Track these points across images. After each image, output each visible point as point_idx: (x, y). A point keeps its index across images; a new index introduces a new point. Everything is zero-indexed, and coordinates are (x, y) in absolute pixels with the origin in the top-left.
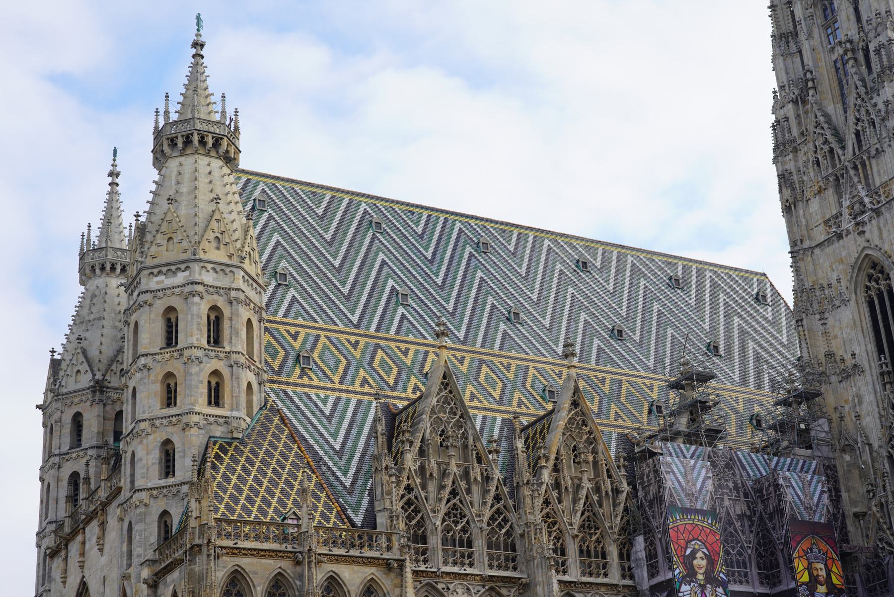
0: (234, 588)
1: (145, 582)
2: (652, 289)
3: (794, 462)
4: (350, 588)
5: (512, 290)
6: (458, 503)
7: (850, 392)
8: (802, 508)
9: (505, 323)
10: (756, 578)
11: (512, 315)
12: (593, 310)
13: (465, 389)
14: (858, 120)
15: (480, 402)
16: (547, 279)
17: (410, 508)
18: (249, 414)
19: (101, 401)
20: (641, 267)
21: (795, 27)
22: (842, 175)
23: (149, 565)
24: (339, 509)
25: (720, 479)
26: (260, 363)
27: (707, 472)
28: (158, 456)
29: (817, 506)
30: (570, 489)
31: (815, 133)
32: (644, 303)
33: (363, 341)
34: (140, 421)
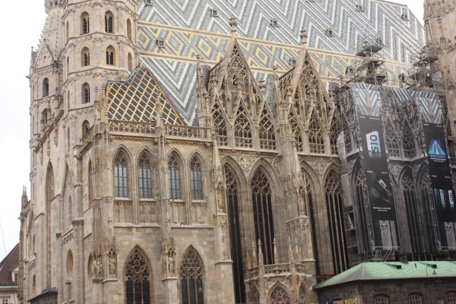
0: (121, 157)
1: (75, 156)
3: (424, 94)
4: (184, 157)
5: (273, 10)
6: (243, 114)
7: (453, 58)
8: (428, 117)
9: (269, 27)
10: (403, 153)
11: (273, 22)
12: (316, 21)
13: (248, 59)
15: (256, 65)
16: (292, 5)
17: (217, 116)
18: (130, 69)
19: (57, 71)
23: (77, 148)
24: (178, 117)
25: (384, 102)
26: (136, 43)
27: (378, 97)
28: (81, 92)
29: (436, 115)
30: (304, 107)
32: (343, 18)
33: (192, 34)
34: (71, 73)
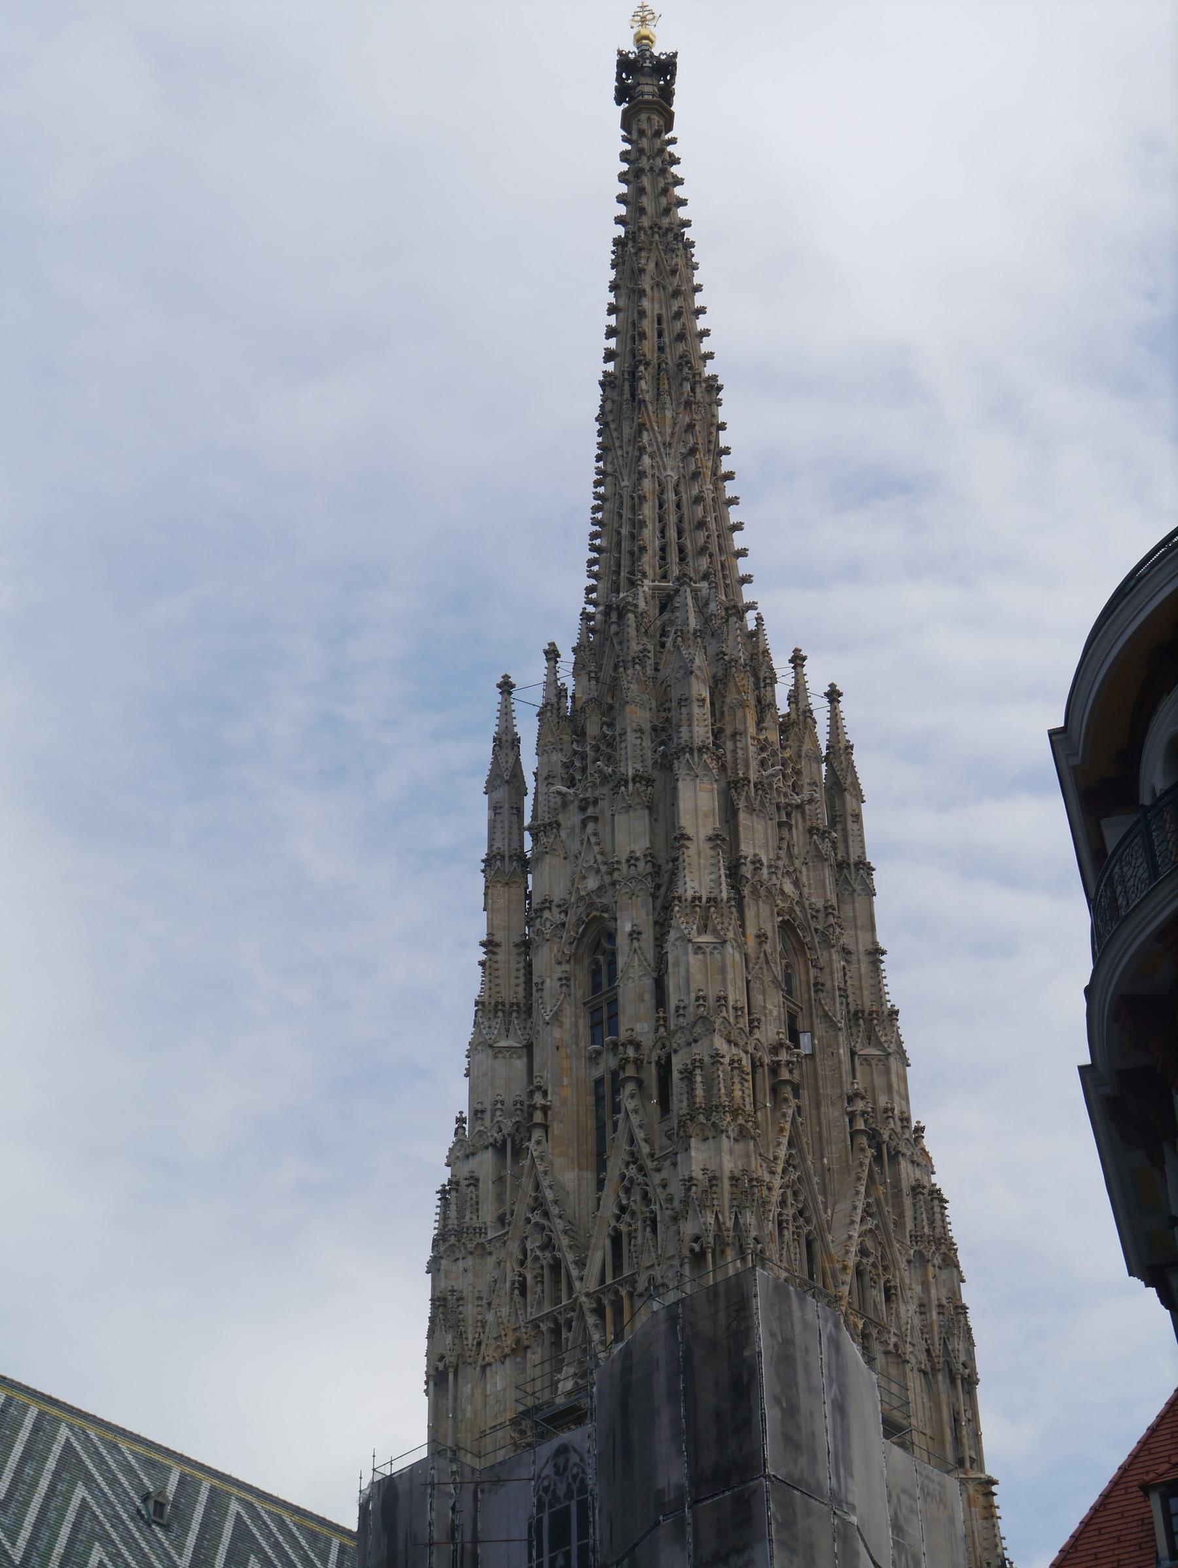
2: (98, 1512)
14: (623, 1209)
20: (84, 1457)
21: (528, 995)
22: (569, 1322)
31: (528, 1221)
32: (71, 1541)
